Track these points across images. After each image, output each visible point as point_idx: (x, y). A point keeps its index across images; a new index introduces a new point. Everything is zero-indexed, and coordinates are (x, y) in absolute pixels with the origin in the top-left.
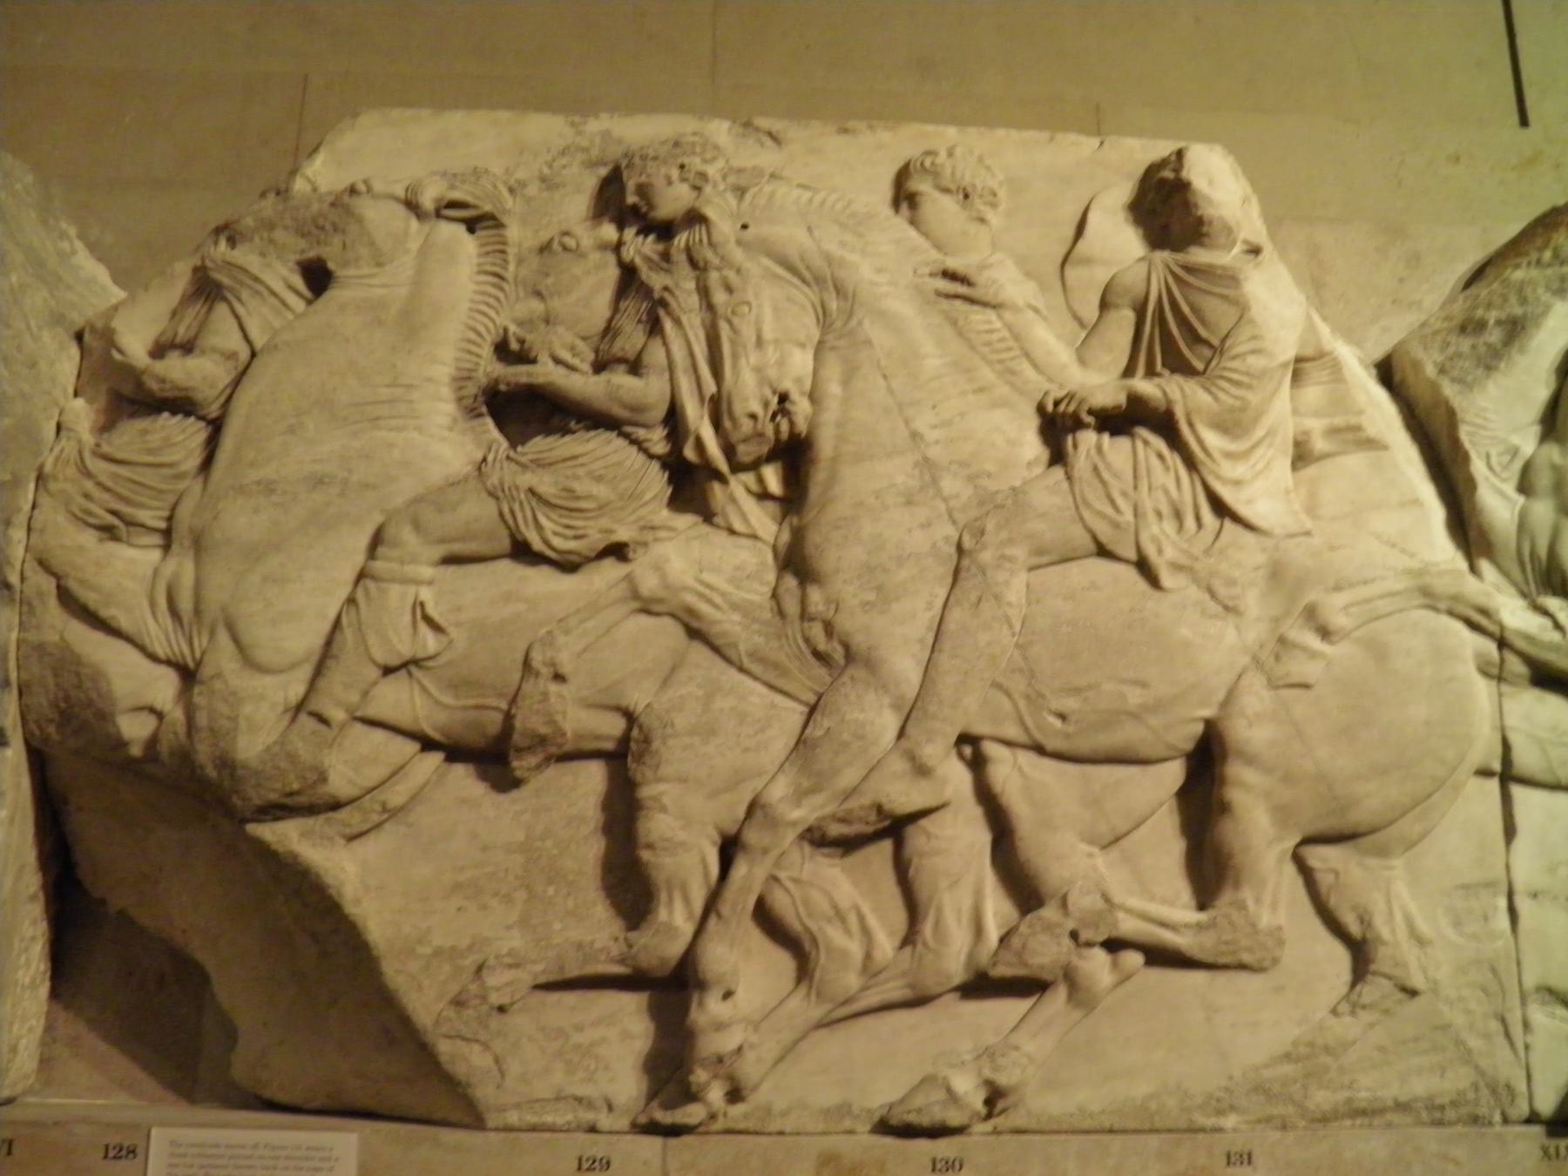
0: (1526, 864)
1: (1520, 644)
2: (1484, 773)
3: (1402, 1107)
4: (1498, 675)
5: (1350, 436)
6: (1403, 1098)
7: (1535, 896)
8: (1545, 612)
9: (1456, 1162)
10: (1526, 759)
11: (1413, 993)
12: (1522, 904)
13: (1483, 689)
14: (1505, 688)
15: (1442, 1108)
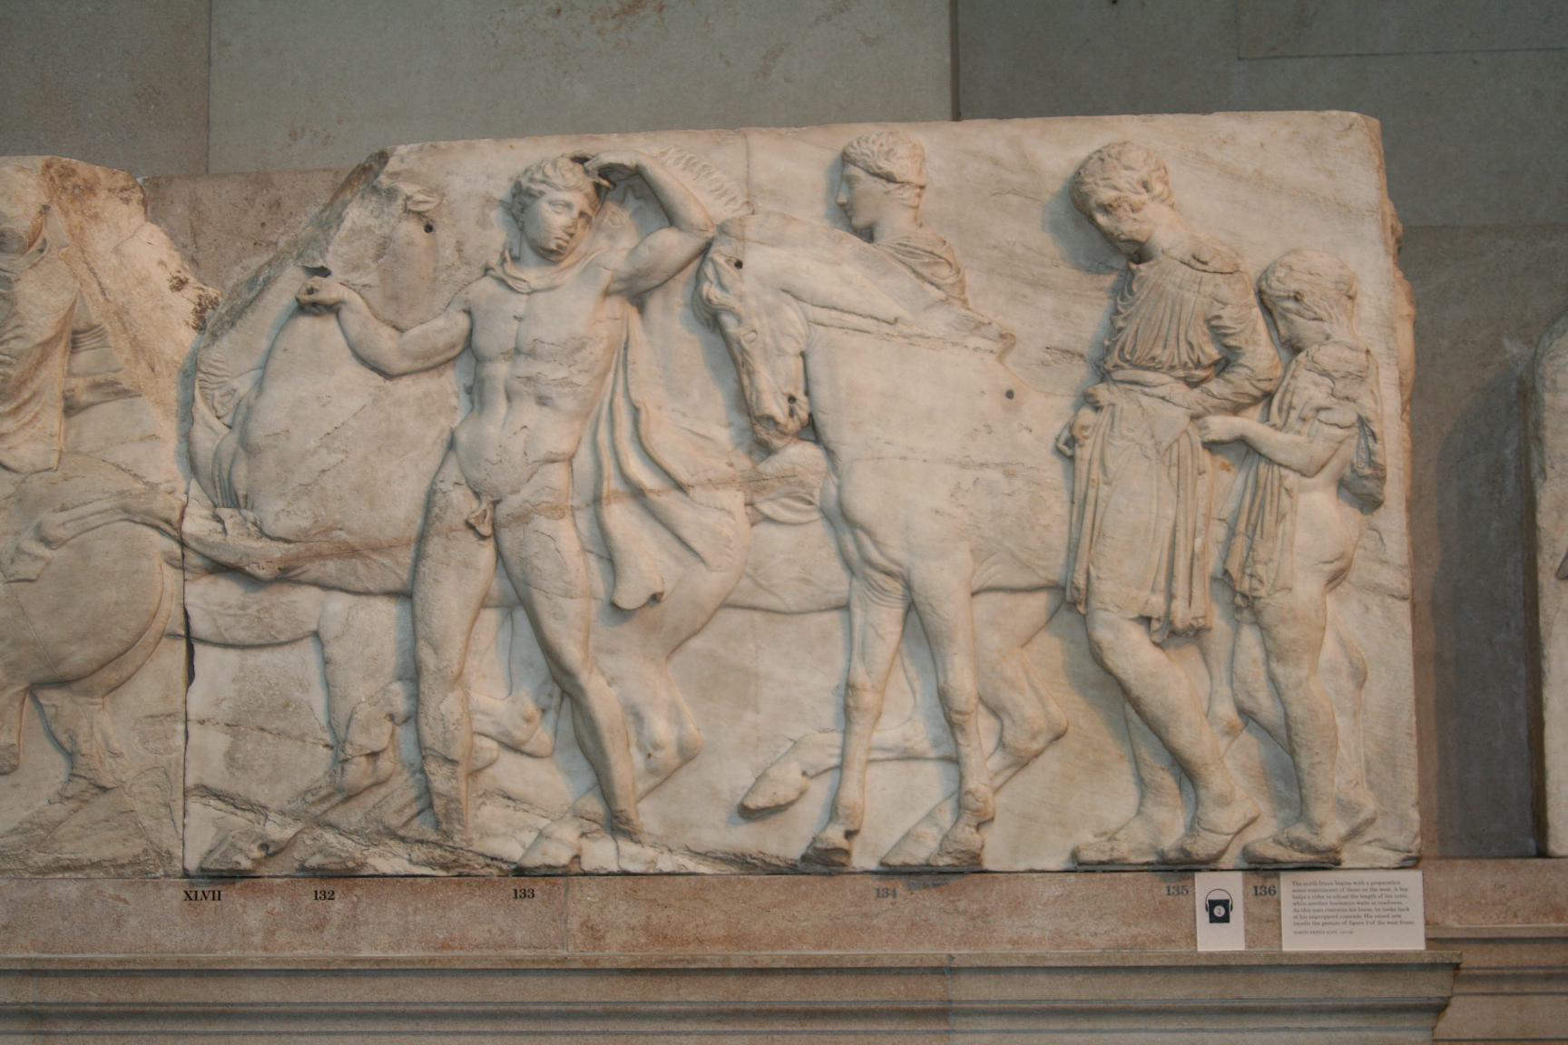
0: (198, 700)
1: (193, 544)
2: (175, 636)
3: (95, 865)
4: (181, 565)
5: (109, 390)
6: (95, 860)
7: (202, 722)
8: (220, 520)
9: (126, 902)
10: (201, 626)
11: (104, 789)
12: (194, 729)
13: (171, 577)
14: (188, 576)
15: (122, 866)
